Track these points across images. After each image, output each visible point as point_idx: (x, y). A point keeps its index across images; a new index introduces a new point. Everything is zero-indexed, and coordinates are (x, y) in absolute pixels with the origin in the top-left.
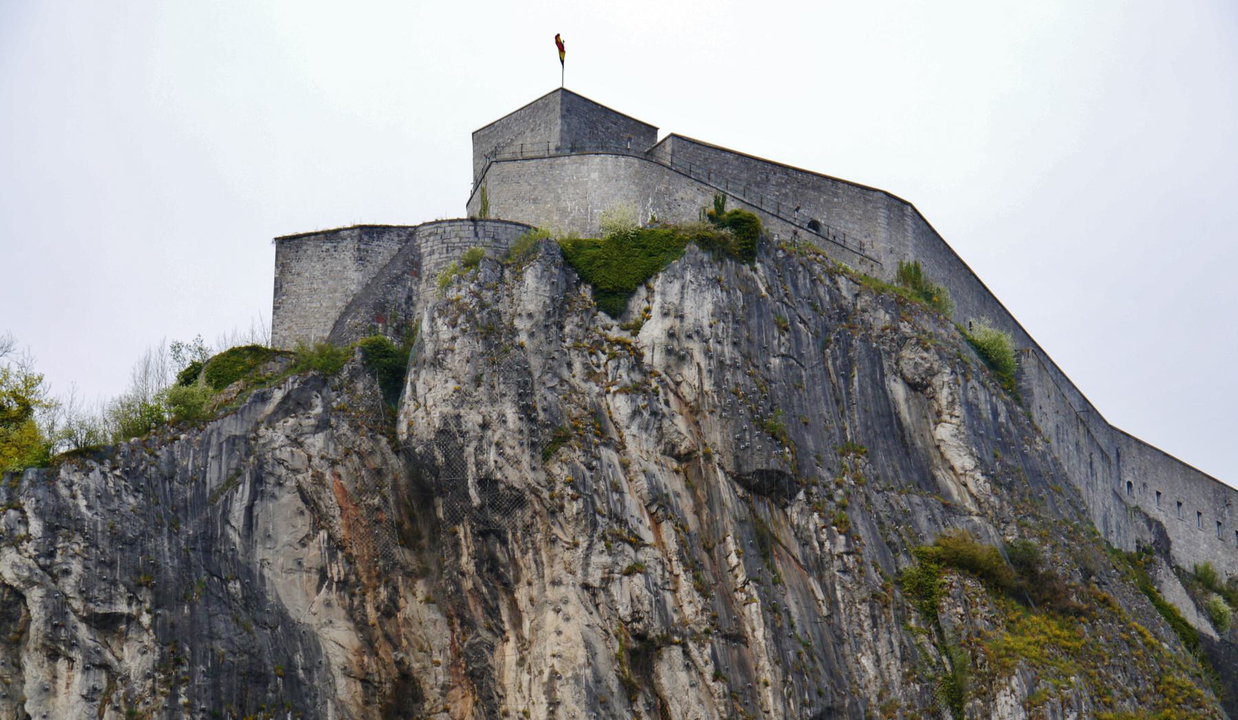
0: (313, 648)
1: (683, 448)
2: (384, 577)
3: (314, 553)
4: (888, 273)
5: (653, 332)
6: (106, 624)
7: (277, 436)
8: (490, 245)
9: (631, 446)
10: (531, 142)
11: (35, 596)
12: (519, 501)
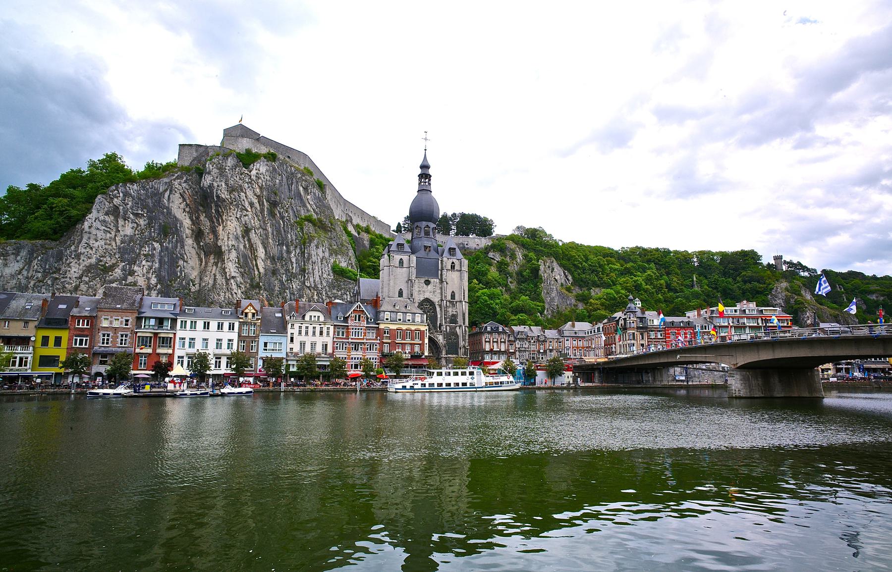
0: (181, 224)
2: (197, 212)
3: (182, 206)
4: (302, 168)
5: (254, 172)
6: (137, 215)
7: (176, 183)
8: (222, 152)
10: (233, 133)
11: (121, 208)
12: (224, 201)
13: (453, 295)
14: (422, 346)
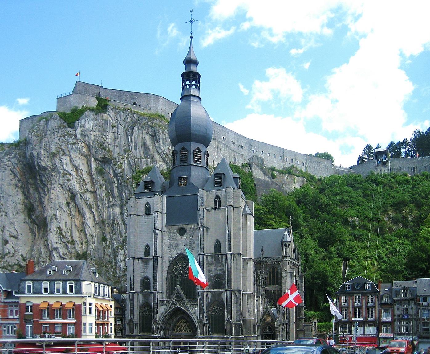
1: (85, 154)
3: (14, 182)
9: (72, 155)
12: (45, 169)
13: (218, 248)
14: (78, 326)
